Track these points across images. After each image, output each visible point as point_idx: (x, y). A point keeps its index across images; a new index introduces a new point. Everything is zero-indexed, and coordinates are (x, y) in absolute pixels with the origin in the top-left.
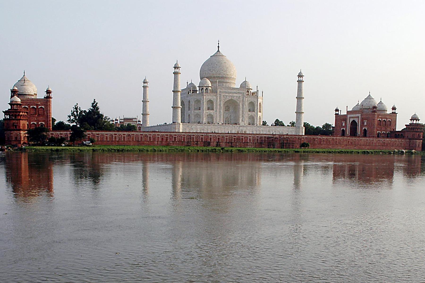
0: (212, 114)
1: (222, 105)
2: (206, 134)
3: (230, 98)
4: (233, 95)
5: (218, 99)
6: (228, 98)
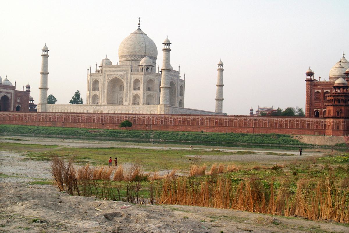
0: (97, 94)
3: (115, 76)
6: (113, 77)
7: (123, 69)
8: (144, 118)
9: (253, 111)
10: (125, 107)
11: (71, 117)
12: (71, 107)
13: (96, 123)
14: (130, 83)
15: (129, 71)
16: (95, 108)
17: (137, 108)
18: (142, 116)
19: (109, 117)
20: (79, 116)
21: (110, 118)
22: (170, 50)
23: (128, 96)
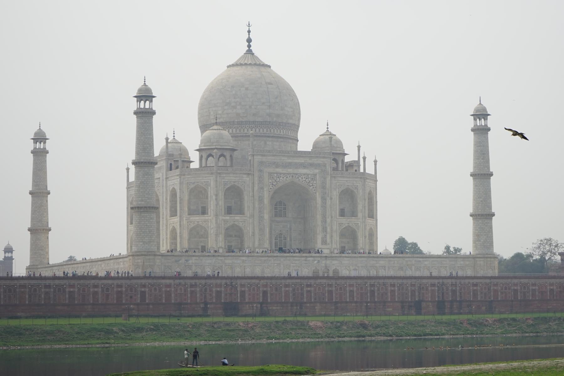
0: (241, 225)
1: (266, 201)
2: (228, 282)
4: (296, 171)
5: (256, 182)
7: (310, 162)
8: (476, 285)
9: (12, 253)
10: (398, 259)
11: (283, 289)
12: (243, 261)
13: (356, 302)
14: (331, 199)
15: (329, 169)
16: (316, 262)
17: (426, 263)
18: (471, 281)
19: (391, 285)
20: (308, 286)
21: (393, 289)
22: (489, 129)
23: (329, 230)
